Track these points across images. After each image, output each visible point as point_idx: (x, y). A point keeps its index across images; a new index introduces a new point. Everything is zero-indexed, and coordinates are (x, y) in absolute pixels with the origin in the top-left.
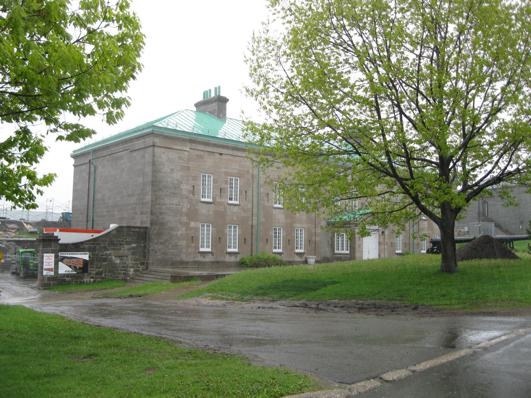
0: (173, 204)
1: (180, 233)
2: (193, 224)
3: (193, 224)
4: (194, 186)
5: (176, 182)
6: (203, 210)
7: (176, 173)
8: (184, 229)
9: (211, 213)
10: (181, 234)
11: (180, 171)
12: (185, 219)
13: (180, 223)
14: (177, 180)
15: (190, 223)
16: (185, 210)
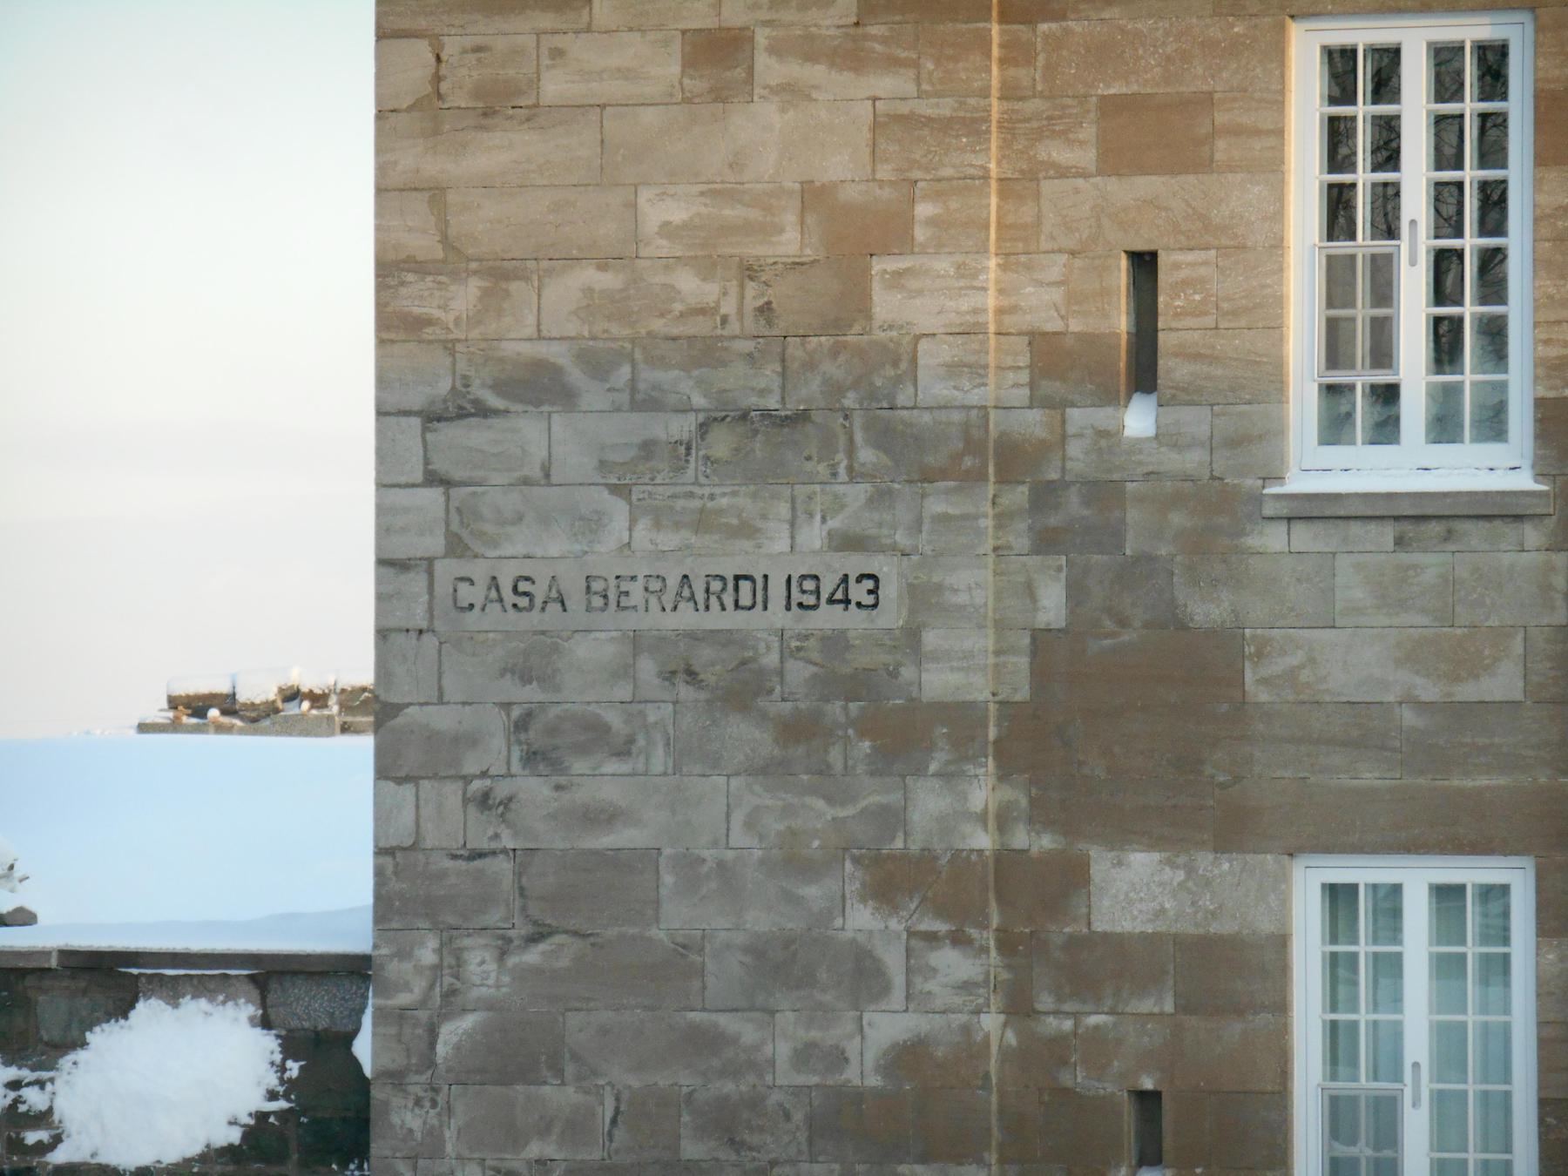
0: (742, 586)
1: (888, 1026)
2: (1134, 889)
3: (1134, 889)
4: (1144, 264)
5: (789, 242)
6: (1341, 650)
7: (792, 93)
8: (953, 964)
9: (1503, 683)
10: (907, 1057)
11: (850, 55)
12: (965, 809)
13: (891, 880)
14: (813, 196)
15: (1075, 875)
16: (965, 667)
